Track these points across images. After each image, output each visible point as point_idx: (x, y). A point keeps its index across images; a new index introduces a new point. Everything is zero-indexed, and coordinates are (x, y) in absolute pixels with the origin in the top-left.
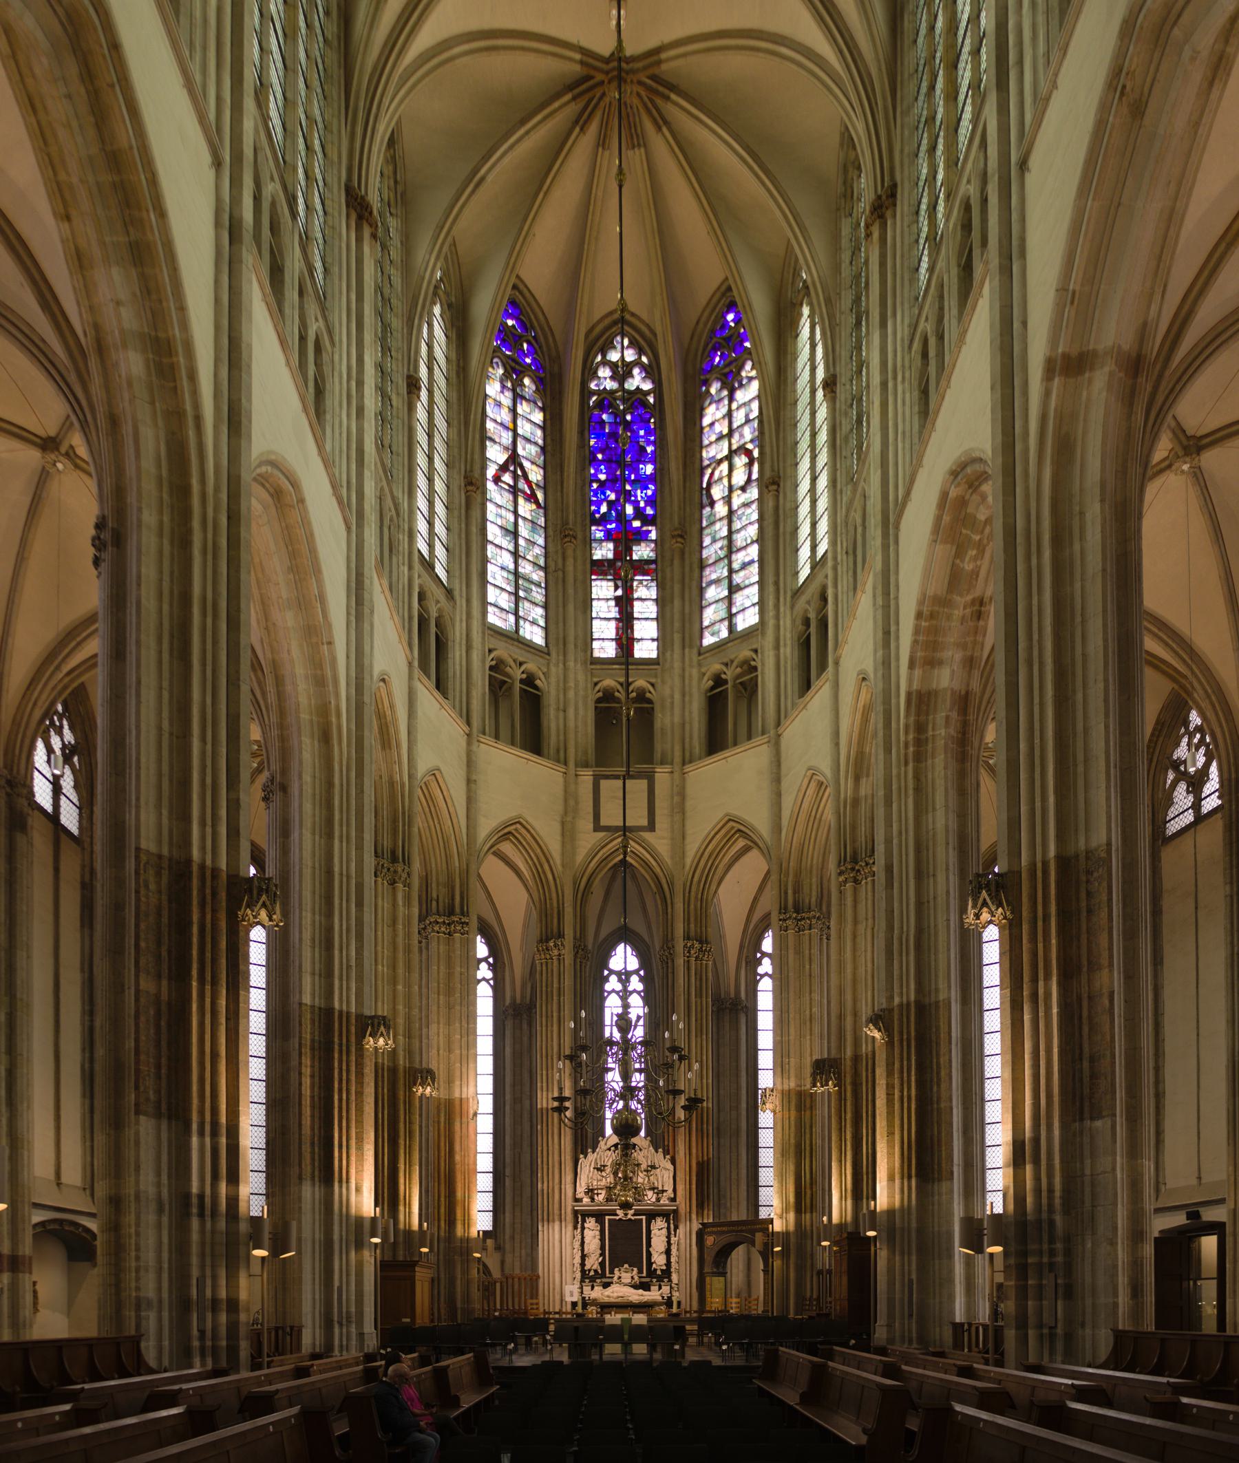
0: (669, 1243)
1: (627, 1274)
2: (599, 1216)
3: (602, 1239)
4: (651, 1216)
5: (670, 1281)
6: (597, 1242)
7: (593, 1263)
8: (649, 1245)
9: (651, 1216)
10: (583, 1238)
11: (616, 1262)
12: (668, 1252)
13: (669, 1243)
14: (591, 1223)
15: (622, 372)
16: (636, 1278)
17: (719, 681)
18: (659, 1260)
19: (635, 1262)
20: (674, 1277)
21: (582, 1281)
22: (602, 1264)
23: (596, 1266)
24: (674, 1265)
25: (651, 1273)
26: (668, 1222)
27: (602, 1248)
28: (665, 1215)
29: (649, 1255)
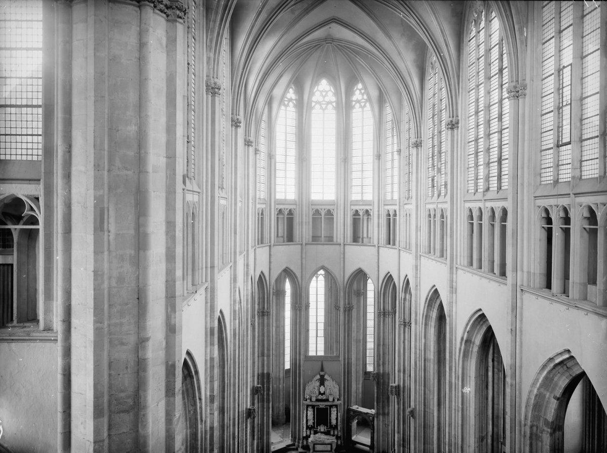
0: (337, 415)
1: (322, 428)
2: (313, 407)
3: (314, 414)
4: (331, 406)
5: (337, 429)
6: (312, 416)
7: (310, 423)
8: (330, 416)
9: (331, 406)
10: (307, 413)
11: (319, 424)
12: (337, 419)
13: (337, 415)
14: (310, 409)
15: (324, 94)
16: (326, 430)
17: (356, 213)
18: (334, 422)
19: (325, 424)
20: (339, 429)
21: (307, 429)
22: (314, 423)
23: (312, 424)
24: (339, 423)
25: (331, 426)
26: (337, 408)
27: (314, 417)
28: (336, 406)
29: (330, 420)
